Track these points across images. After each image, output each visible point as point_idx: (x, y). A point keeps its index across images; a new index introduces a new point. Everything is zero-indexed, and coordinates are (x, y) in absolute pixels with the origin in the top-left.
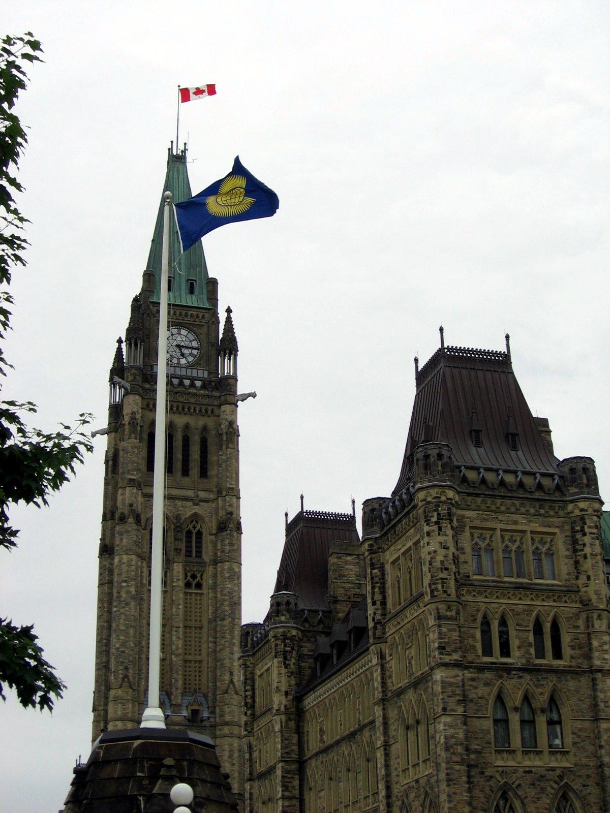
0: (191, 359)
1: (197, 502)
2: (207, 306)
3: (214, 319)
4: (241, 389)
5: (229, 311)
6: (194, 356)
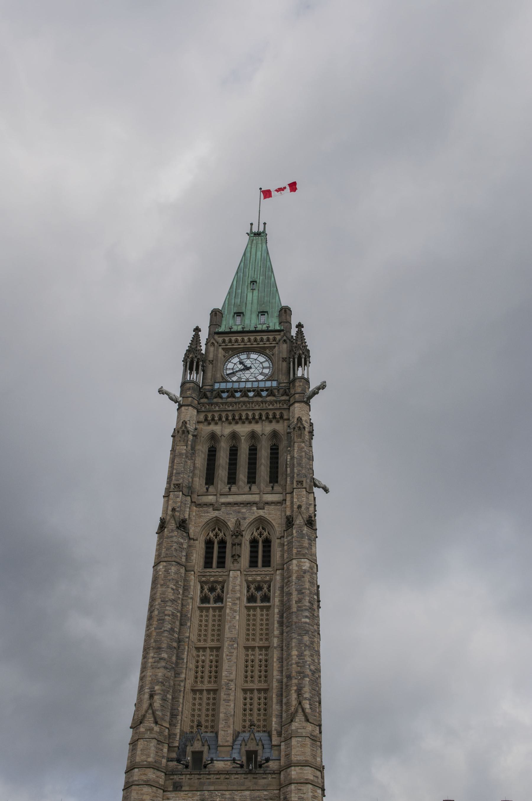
2: (278, 328)
3: (285, 338)
5: (300, 326)
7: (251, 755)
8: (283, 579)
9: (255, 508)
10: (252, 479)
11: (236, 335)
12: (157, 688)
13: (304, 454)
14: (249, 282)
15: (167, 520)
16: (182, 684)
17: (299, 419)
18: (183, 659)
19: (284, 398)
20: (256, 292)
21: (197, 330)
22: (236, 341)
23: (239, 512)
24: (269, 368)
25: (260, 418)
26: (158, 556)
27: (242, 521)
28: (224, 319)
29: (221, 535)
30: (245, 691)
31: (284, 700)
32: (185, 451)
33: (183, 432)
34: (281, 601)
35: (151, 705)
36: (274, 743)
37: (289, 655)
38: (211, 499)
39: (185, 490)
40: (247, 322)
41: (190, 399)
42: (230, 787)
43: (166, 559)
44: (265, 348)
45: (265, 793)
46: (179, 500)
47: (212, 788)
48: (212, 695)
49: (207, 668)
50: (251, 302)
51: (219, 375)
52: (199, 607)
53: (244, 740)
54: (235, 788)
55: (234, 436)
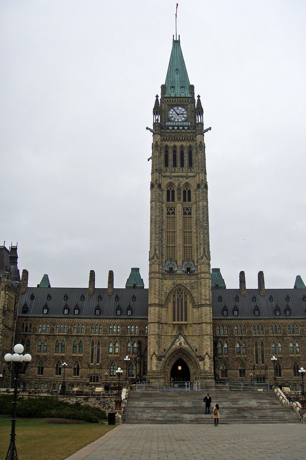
0: (183, 119)
1: (187, 177)
3: (192, 101)
4: (205, 128)
5: (199, 96)
6: (185, 118)
7: (188, 269)
8: (197, 208)
9: (185, 179)
10: (182, 165)
11: (172, 98)
12: (157, 247)
13: (203, 158)
15: (154, 184)
16: (164, 245)
17: (201, 142)
18: (164, 236)
19: (193, 131)
20: (178, 74)
21: (157, 96)
22: (173, 101)
23: (179, 180)
24: (186, 114)
25: (185, 139)
26: (152, 198)
27: (180, 184)
28: (166, 89)
29: (173, 188)
30: (184, 247)
31: (199, 251)
32: (158, 155)
34: (196, 216)
35: (155, 253)
36: (195, 265)
37: (200, 237)
38: (168, 174)
39: (159, 171)
40: (176, 92)
41: (158, 131)
42: (182, 279)
43: (156, 200)
45: (194, 281)
46: (157, 176)
47: (177, 279)
48: (173, 248)
49: (171, 239)
51: (167, 117)
52: (167, 217)
53: (186, 264)
54: (184, 279)
55: (175, 146)
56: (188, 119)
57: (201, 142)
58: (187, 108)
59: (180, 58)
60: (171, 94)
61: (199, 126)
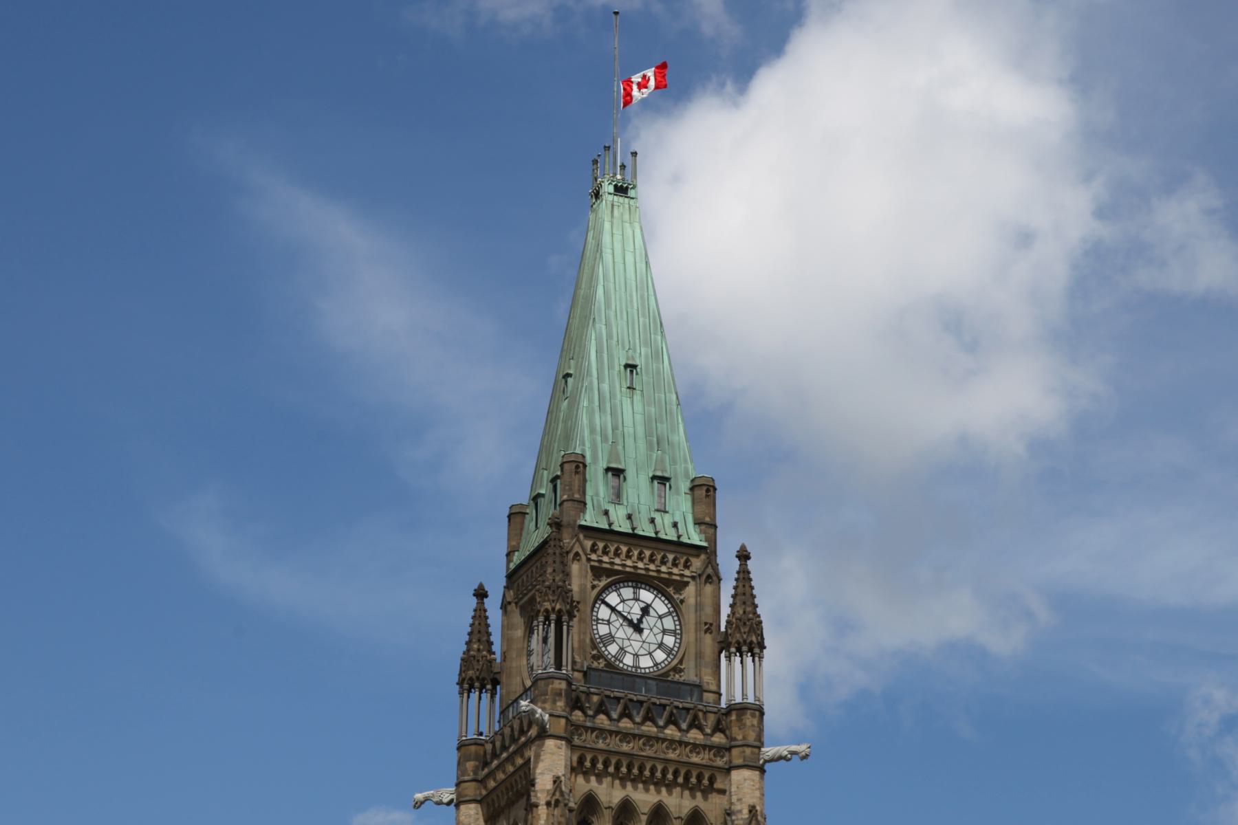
0: (660, 656)
2: (695, 537)
3: (709, 571)
5: (744, 556)
11: (617, 538)
14: (623, 363)
20: (637, 397)
33: (557, 802)
44: (668, 582)
50: (631, 430)
51: (588, 641)
56: (681, 662)
57: (752, 810)
58: (682, 601)
59: (642, 297)
60: (611, 508)
61: (748, 723)
